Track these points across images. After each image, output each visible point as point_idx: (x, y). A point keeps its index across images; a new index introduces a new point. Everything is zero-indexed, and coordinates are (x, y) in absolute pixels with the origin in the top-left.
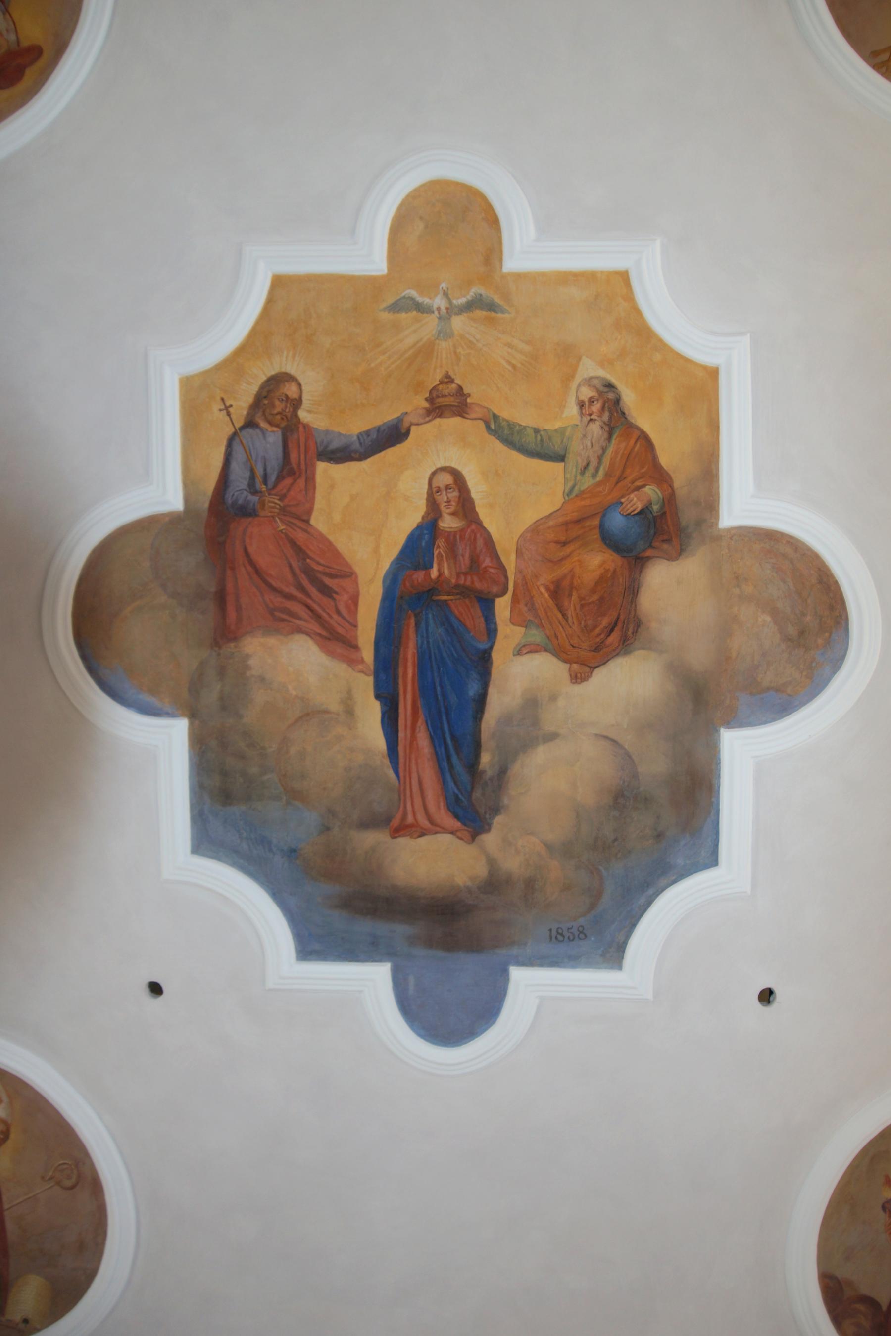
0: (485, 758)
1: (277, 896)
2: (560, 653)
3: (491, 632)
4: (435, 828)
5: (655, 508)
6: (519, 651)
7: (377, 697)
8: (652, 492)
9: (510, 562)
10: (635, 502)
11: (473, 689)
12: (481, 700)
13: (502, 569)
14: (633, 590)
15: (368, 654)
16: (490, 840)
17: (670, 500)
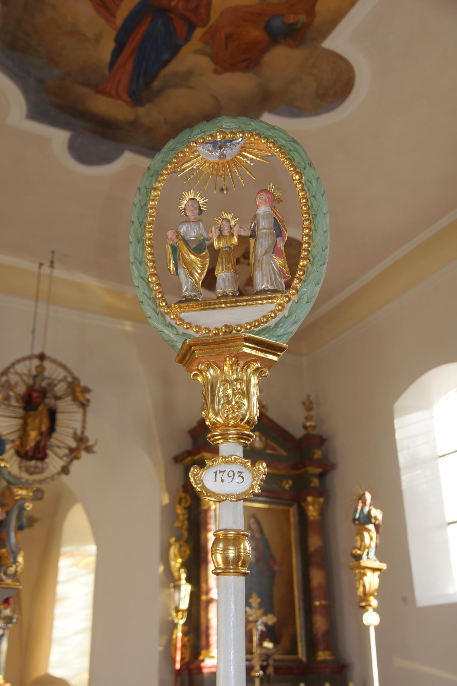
0: (156, 84)
1: (26, 91)
2: (214, 59)
3: (187, 39)
4: (118, 96)
5: (299, 25)
6: (197, 52)
7: (116, 40)
8: (302, 18)
9: (214, 16)
10: (291, 19)
11: (165, 57)
12: (166, 63)
13: (208, 17)
14: (264, 51)
15: (119, 21)
16: (141, 111)
17: (307, 26)
